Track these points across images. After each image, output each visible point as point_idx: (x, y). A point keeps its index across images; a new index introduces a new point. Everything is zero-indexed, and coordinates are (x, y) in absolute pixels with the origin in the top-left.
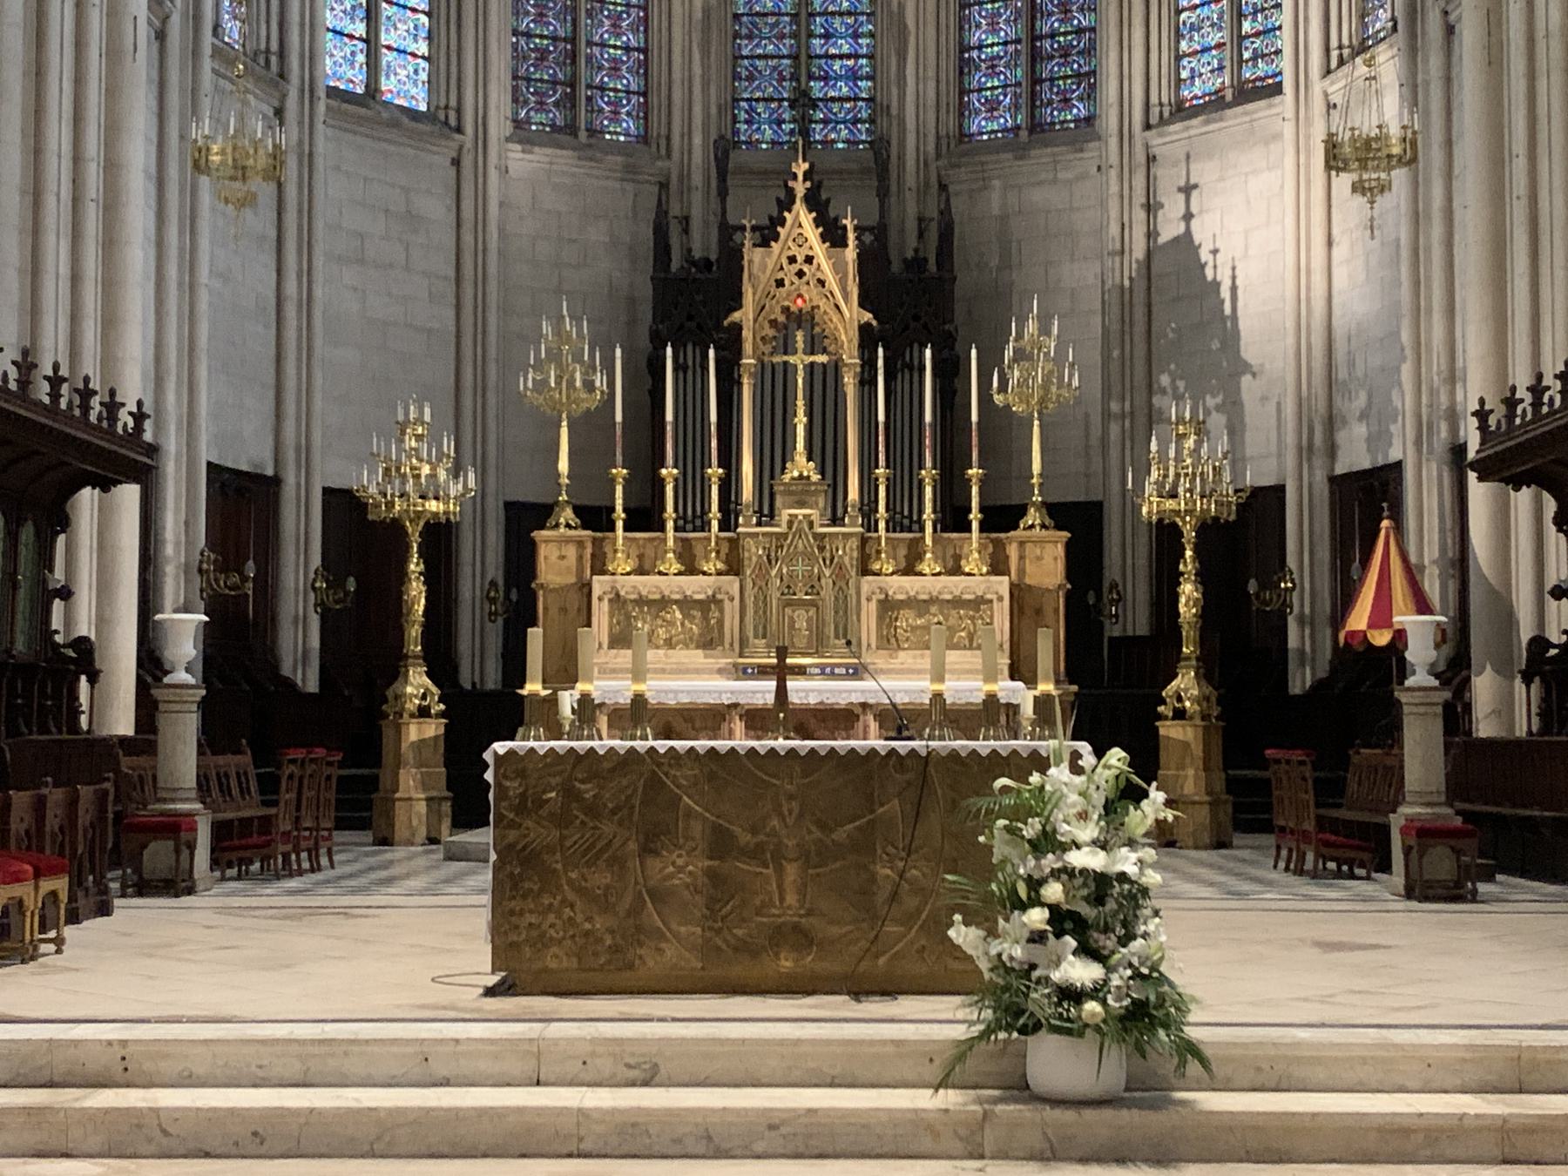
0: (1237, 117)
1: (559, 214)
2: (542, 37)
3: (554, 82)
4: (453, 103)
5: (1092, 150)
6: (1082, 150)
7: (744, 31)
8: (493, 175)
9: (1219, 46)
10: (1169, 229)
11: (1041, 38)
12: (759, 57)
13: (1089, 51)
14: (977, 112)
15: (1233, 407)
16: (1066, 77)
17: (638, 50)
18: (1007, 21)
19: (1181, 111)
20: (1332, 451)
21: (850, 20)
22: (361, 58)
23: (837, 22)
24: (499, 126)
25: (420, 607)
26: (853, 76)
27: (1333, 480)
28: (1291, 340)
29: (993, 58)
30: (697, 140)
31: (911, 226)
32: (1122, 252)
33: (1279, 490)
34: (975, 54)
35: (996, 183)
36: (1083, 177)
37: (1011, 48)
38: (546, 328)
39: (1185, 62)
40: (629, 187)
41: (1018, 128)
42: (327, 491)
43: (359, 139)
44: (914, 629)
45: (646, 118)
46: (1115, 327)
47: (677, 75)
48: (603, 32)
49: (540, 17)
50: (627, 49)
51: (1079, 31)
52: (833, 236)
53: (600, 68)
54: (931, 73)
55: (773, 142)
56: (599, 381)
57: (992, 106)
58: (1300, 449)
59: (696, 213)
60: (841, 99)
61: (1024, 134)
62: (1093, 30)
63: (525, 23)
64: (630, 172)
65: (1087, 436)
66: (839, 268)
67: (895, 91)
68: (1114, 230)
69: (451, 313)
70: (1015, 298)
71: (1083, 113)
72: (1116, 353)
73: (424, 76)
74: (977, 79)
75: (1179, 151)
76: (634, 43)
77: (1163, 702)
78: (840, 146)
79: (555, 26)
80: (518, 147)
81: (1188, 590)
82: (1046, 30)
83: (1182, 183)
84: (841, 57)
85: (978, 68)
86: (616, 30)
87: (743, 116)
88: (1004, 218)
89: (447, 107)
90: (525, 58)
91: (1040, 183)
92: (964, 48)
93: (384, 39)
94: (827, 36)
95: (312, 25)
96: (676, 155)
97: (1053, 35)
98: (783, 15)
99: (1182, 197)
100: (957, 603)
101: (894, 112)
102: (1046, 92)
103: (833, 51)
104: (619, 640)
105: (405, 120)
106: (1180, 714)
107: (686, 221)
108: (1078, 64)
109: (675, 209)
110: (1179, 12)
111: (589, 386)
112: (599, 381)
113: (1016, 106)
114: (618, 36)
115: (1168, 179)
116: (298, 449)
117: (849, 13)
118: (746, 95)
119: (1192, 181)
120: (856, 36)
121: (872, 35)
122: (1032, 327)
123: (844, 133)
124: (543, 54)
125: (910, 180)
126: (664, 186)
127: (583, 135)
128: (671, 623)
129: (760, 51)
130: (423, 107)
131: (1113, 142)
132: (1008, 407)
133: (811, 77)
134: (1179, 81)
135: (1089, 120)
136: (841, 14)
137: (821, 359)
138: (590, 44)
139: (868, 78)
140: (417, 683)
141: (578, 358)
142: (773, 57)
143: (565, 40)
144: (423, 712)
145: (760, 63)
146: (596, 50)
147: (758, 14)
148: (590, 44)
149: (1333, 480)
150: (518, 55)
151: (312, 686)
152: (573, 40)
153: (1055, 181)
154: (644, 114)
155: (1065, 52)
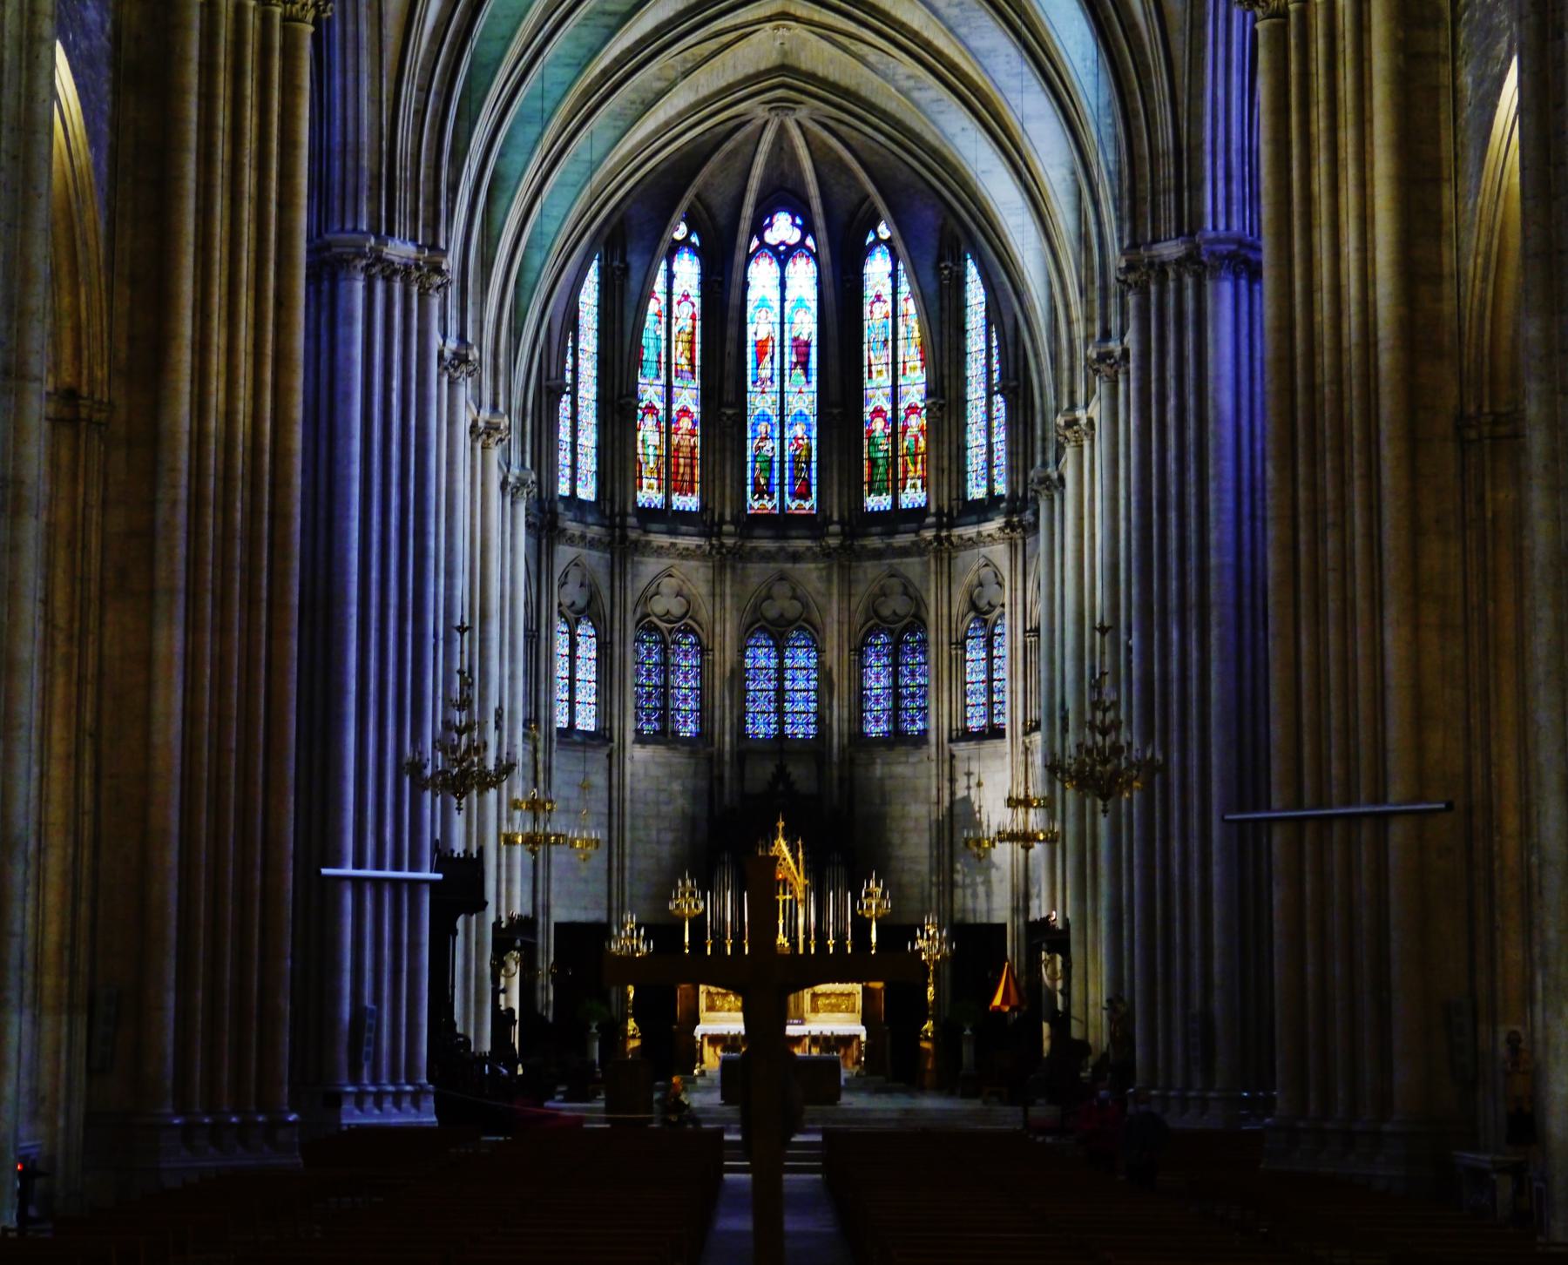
0: (989, 746)
1: (658, 777)
2: (649, 686)
3: (655, 709)
4: (608, 726)
5: (921, 754)
6: (920, 748)
7: (751, 677)
8: (628, 762)
9: (983, 704)
10: (961, 793)
11: (901, 687)
12: (759, 690)
13: (923, 697)
14: (870, 722)
15: (988, 882)
16: (913, 709)
17: (697, 688)
18: (884, 677)
19: (966, 735)
20: (1027, 910)
21: (805, 672)
22: (566, 710)
23: (798, 672)
24: (630, 736)
25: (632, 996)
26: (807, 700)
27: (1027, 923)
28: (1008, 858)
29: (878, 695)
30: (727, 738)
31: (835, 782)
32: (938, 803)
33: (1004, 926)
34: (868, 692)
35: (878, 761)
36: (921, 761)
37: (887, 691)
38: (680, 883)
39: (969, 708)
40: (692, 761)
41: (889, 732)
42: (557, 925)
43: (570, 753)
44: (825, 1005)
45: (700, 723)
46: (934, 841)
47: (717, 703)
48: (680, 681)
49: (649, 677)
50: (691, 689)
51: (920, 686)
52: (794, 851)
53: (678, 699)
54: (846, 703)
55: (765, 734)
56: (701, 906)
57: (877, 720)
58: (1013, 909)
59: (727, 774)
60: (801, 713)
61: (892, 737)
62: (926, 686)
63: (643, 680)
64: (693, 754)
65: (922, 893)
66: (796, 862)
67: (827, 712)
68: (934, 792)
69: (606, 832)
70: (888, 821)
71: (922, 727)
72: (935, 853)
73: (593, 713)
74: (870, 704)
75: (965, 754)
76: (694, 685)
77: (921, 1033)
78: (800, 736)
79: (655, 680)
80: (638, 746)
81: (931, 989)
82: (903, 684)
83: (966, 770)
84: (800, 691)
85: (870, 699)
86: (686, 680)
87: (750, 721)
88: (882, 779)
89: (605, 729)
90: (642, 697)
91: (900, 763)
92: (862, 688)
93: (578, 698)
94: (793, 680)
95: (550, 707)
96: (716, 745)
97: (907, 686)
98: (769, 669)
99: (965, 778)
100: (842, 994)
101: (827, 722)
102: (904, 715)
103: (796, 688)
104: (711, 1008)
105: (589, 741)
106: (927, 1039)
107: (721, 778)
108: (919, 702)
109: (716, 771)
110: (966, 683)
111: (696, 906)
112: (701, 906)
113: (888, 721)
114: (686, 682)
115: (961, 767)
116: (544, 905)
117: (805, 668)
118: (751, 710)
119: (971, 770)
120: (808, 680)
121: (816, 679)
122: (872, 884)
123: (802, 730)
124: (649, 694)
125: (835, 758)
126: (710, 759)
127: (670, 736)
128: (730, 1002)
129: (758, 687)
130: (593, 729)
131: (933, 749)
132: (863, 915)
133: (785, 701)
134: (966, 718)
135: (925, 732)
136: (801, 669)
137: (788, 897)
138: (673, 688)
139: (814, 701)
140: (631, 1024)
141: (692, 894)
142: (765, 690)
143: (661, 687)
144: (633, 1037)
145: (759, 694)
146: (676, 691)
147: (758, 668)
148: (673, 688)
149: (1027, 923)
150: (639, 697)
151: (550, 1018)
152: (666, 685)
153: (907, 762)
154: (701, 721)
155: (913, 695)
